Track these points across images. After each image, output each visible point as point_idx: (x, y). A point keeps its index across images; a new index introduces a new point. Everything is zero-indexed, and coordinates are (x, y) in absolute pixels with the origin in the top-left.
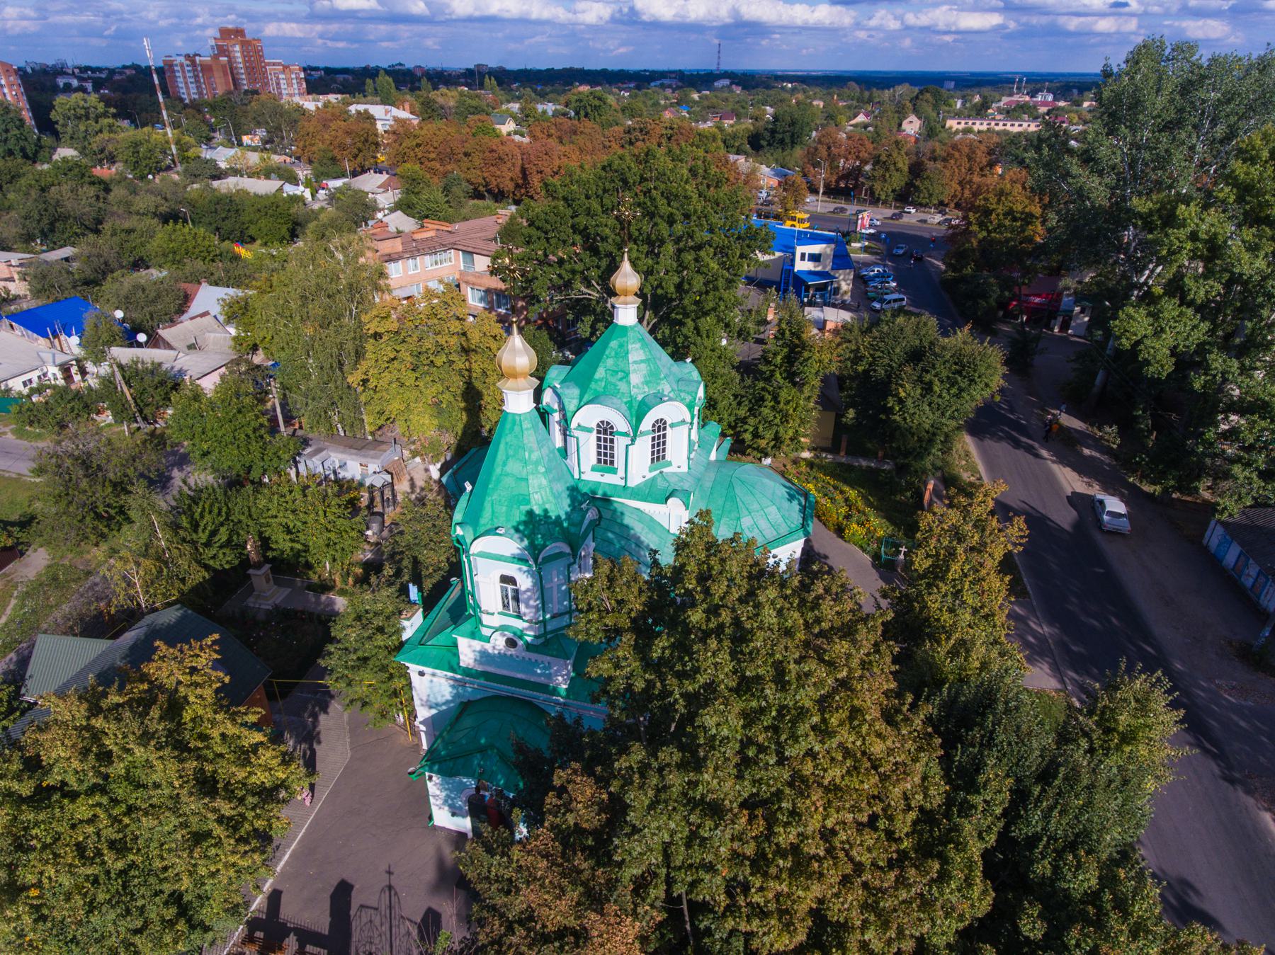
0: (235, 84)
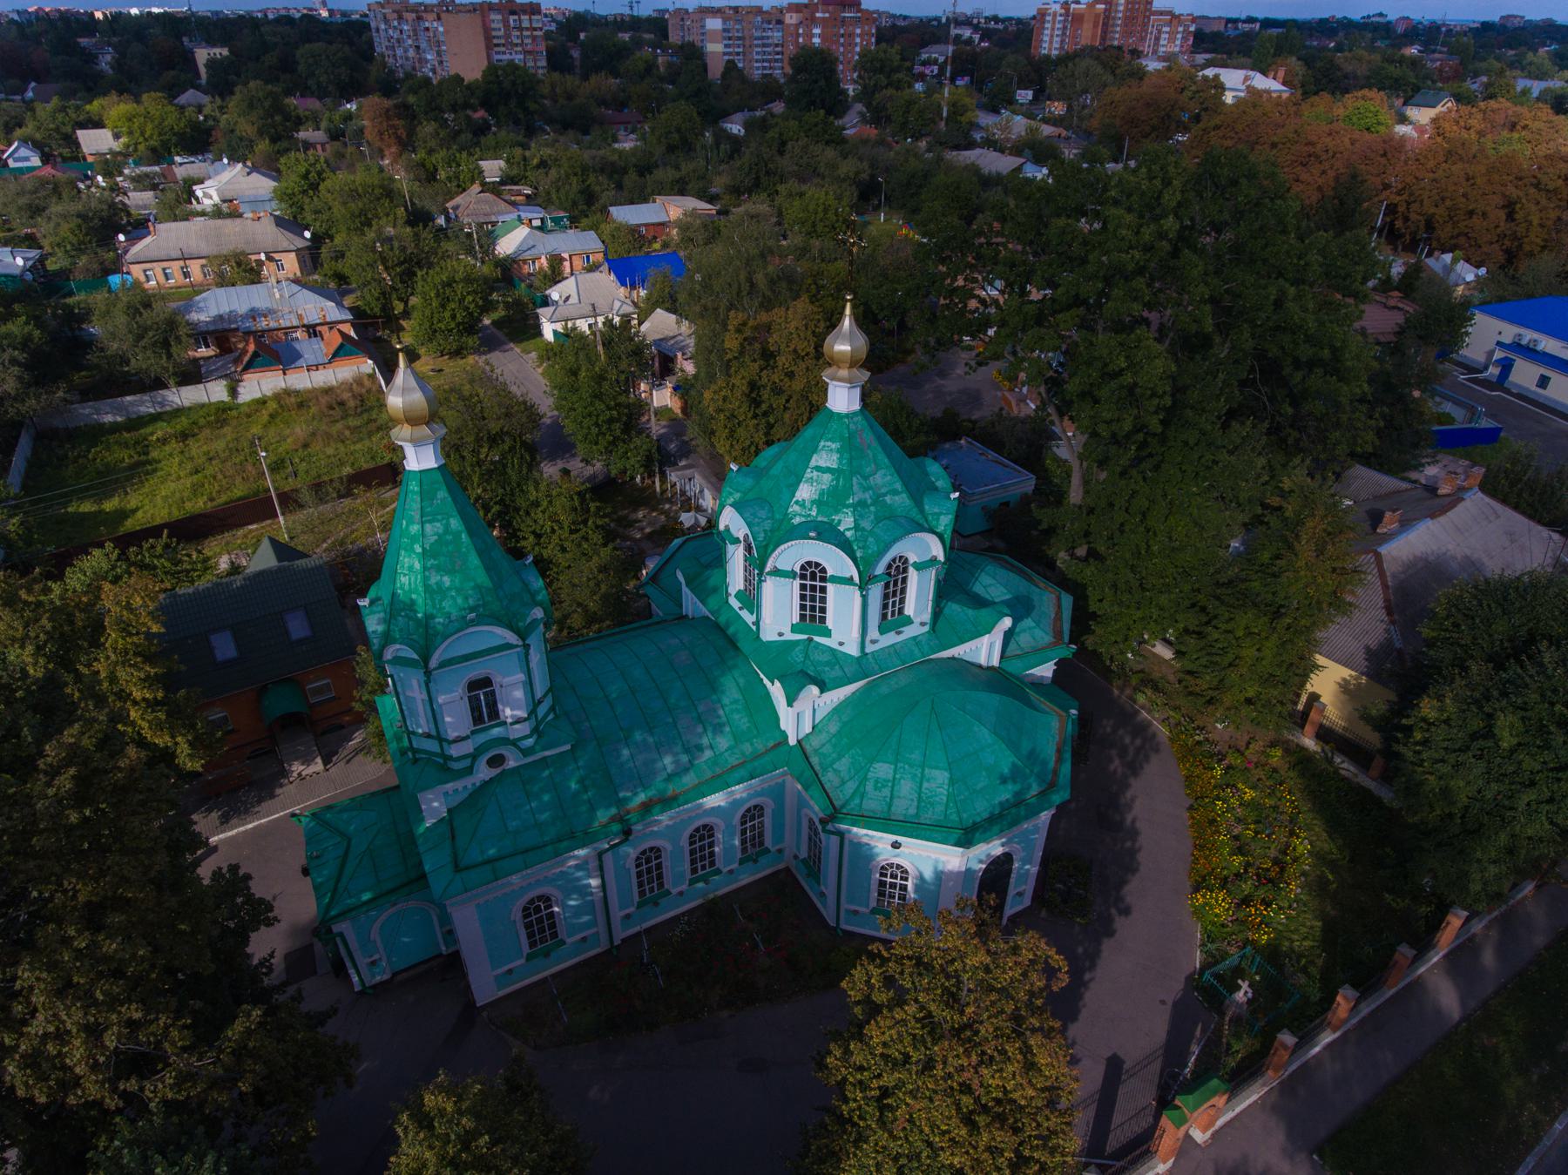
0: (1103, 39)
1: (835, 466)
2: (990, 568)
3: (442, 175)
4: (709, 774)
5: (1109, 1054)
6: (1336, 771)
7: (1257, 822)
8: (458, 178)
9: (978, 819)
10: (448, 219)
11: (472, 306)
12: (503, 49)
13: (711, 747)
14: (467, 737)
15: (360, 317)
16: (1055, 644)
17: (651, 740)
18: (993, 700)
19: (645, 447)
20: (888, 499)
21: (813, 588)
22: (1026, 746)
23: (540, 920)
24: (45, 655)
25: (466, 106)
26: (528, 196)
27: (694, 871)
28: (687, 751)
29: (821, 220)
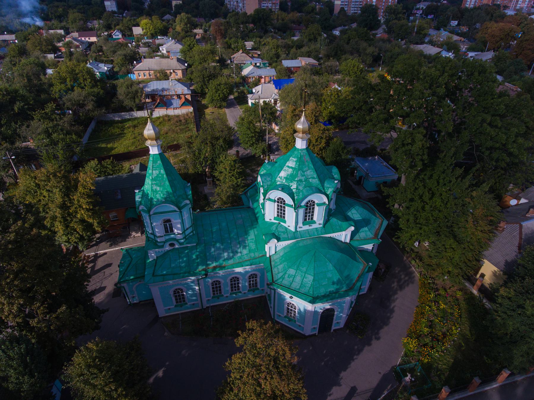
1: (294, 166)
2: (357, 207)
3: (233, 46)
4: (238, 261)
5: (352, 385)
6: (483, 305)
7: (442, 317)
8: (237, 47)
9: (320, 295)
10: (231, 61)
11: (225, 93)
12: (265, 2)
13: (241, 253)
14: (162, 236)
15: (194, 93)
16: (373, 238)
17: (222, 247)
18: (338, 255)
19: (262, 147)
21: (281, 206)
22: (346, 273)
23: (179, 296)
24: (62, 192)
25: (246, 23)
26: (259, 55)
27: (232, 290)
28: (232, 252)
29: (352, 70)
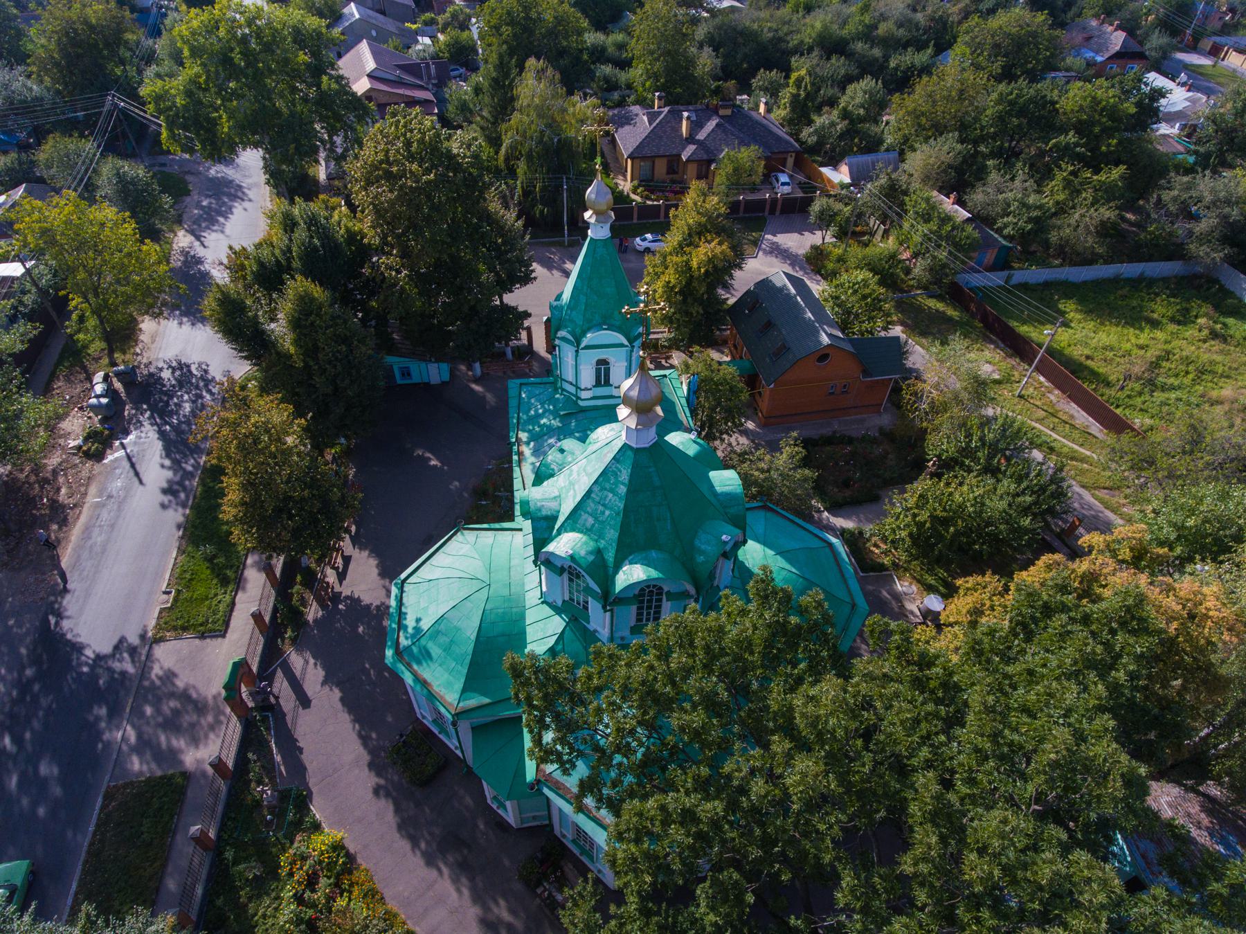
20: (572, 492)
22: (435, 651)
